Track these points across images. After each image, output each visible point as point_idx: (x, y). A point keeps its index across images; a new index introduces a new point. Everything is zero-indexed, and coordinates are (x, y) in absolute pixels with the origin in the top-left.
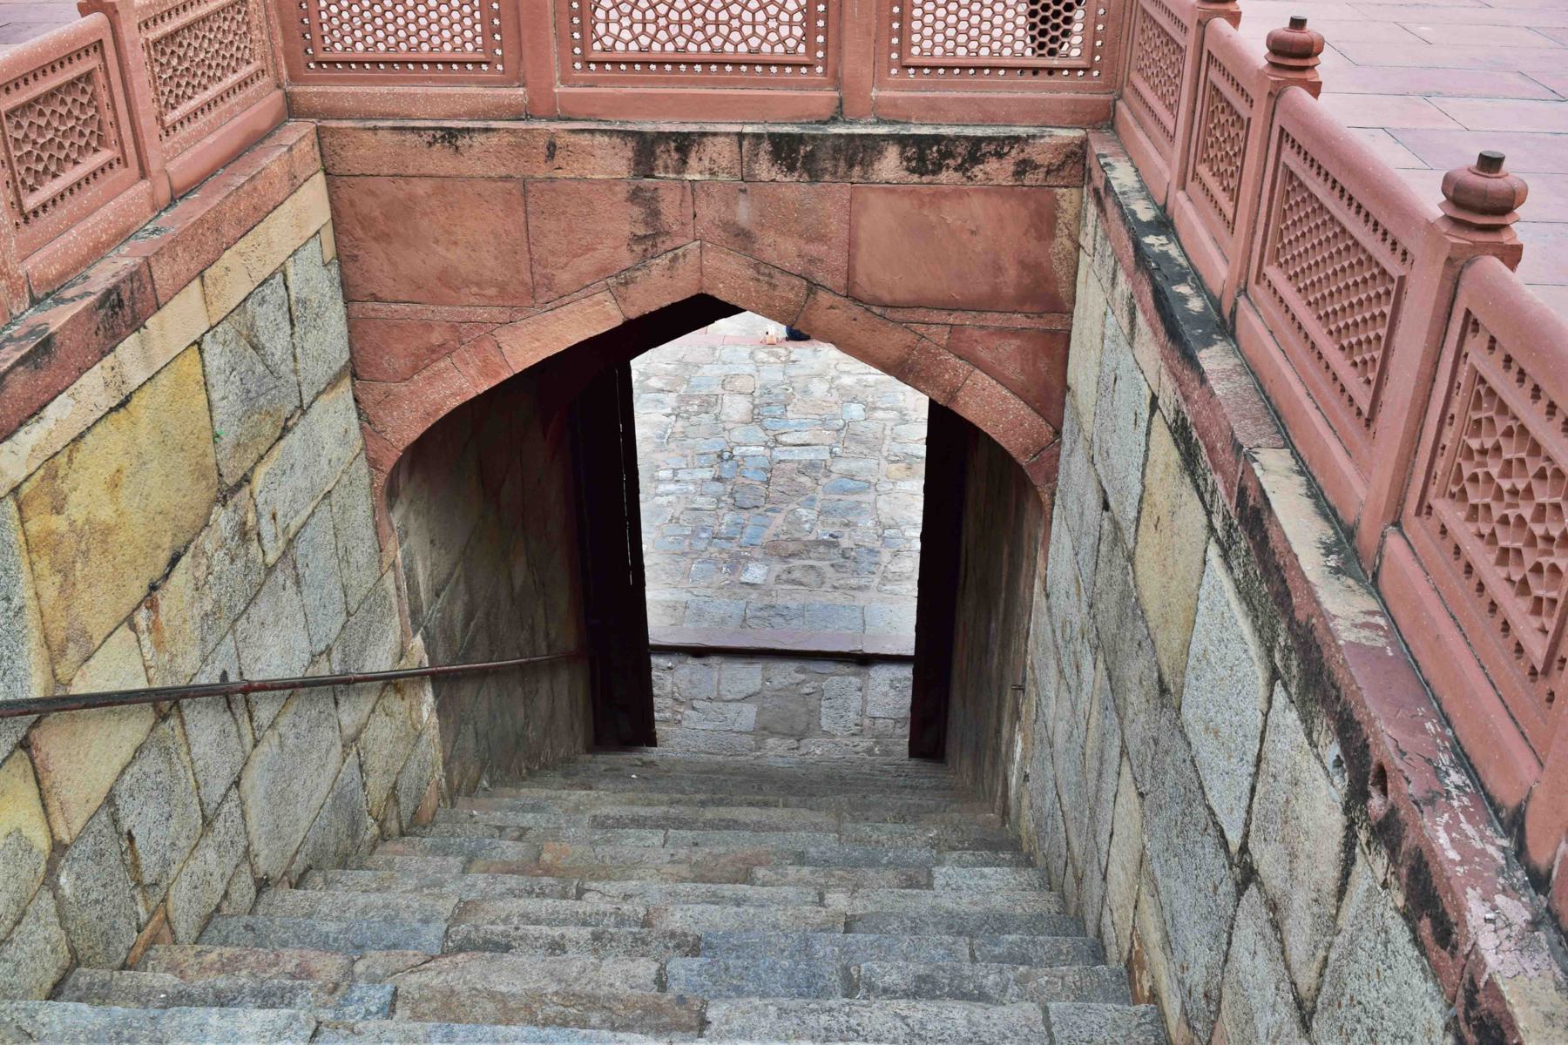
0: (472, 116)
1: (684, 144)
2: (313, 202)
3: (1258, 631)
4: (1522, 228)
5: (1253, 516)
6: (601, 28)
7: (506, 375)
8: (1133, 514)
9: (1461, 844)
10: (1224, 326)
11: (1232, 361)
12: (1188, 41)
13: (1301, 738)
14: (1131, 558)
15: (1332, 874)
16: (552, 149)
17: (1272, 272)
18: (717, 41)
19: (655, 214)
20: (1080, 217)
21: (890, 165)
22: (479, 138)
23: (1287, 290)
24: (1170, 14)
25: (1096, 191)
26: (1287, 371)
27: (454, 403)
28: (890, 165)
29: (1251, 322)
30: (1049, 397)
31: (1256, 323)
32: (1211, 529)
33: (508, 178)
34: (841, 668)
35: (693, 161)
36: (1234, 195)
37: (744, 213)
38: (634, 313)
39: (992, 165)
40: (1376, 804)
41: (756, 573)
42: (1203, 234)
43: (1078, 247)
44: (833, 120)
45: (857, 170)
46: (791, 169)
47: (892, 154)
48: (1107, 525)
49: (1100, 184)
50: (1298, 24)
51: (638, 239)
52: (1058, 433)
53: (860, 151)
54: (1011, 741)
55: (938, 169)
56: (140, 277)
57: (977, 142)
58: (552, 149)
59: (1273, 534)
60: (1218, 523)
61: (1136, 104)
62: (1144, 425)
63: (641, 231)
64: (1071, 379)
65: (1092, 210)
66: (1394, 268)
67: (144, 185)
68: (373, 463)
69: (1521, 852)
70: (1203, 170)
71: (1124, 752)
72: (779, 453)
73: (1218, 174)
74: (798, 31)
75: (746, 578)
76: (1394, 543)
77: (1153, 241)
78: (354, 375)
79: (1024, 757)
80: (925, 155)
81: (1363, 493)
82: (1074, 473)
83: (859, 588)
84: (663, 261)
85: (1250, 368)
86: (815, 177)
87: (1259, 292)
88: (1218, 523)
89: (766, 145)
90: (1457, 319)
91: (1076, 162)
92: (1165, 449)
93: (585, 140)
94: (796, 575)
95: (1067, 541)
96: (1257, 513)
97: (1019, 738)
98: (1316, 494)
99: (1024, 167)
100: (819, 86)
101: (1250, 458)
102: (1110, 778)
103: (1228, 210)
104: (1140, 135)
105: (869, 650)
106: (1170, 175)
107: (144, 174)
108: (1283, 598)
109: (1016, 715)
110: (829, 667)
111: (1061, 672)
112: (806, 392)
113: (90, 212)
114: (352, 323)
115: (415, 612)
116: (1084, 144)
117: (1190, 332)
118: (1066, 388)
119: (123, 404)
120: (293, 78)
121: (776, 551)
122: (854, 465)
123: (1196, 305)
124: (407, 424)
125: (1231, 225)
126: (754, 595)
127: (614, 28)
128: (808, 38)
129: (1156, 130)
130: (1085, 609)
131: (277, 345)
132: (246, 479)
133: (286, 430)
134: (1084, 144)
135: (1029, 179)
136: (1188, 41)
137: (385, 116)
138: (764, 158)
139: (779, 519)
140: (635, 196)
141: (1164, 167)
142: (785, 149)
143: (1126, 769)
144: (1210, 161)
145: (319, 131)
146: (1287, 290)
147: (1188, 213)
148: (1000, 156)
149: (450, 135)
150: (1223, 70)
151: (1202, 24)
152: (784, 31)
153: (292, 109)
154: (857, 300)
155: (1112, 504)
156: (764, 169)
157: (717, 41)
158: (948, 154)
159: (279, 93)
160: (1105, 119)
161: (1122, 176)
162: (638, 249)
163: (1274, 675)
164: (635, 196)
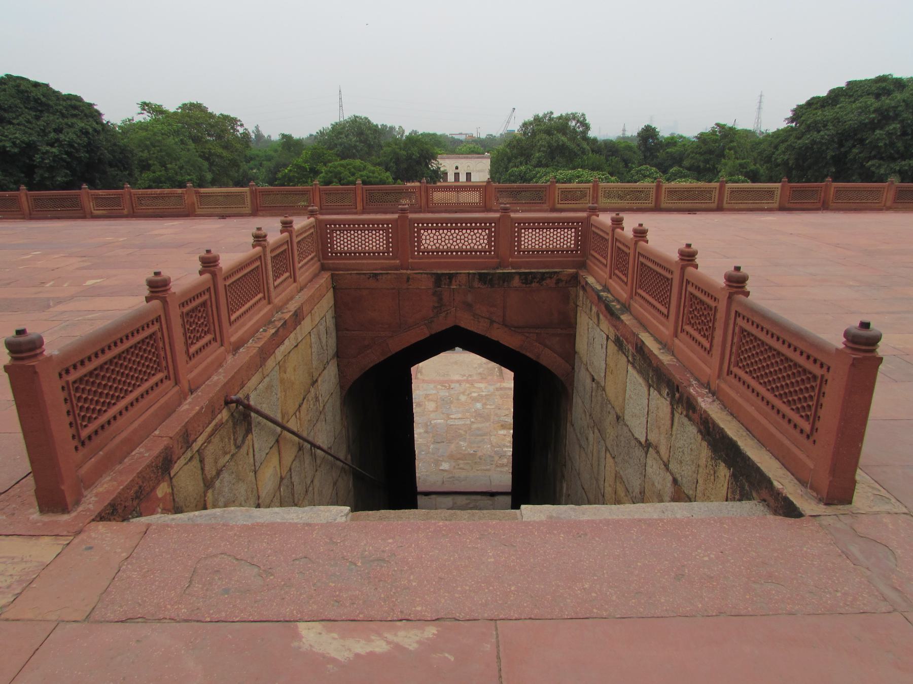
0: (382, 269)
1: (451, 277)
2: (329, 297)
3: (644, 379)
4: (698, 260)
5: (641, 348)
6: (424, 242)
7: (389, 354)
8: (603, 375)
9: (697, 392)
10: (626, 308)
11: (630, 317)
12: (609, 237)
13: (659, 396)
14: (604, 390)
15: (669, 423)
16: (408, 279)
17: (640, 291)
18: (460, 245)
19: (440, 299)
20: (577, 296)
21: (516, 282)
22: (384, 276)
23: (644, 294)
24: (602, 230)
25: (583, 287)
26: (646, 314)
27: (371, 365)
28: (516, 282)
29: (636, 306)
30: (570, 354)
31: (636, 305)
32: (629, 361)
33: (394, 289)
34: (484, 497)
35: (453, 282)
36: (626, 275)
37: (470, 298)
38: (433, 332)
39: (548, 281)
40: (677, 395)
41: (445, 466)
42: (618, 288)
43: (577, 306)
44: (497, 268)
45: (506, 284)
46: (485, 284)
47: (517, 278)
48: (594, 385)
49: (583, 283)
50: (641, 225)
51: (435, 308)
52: (573, 368)
53: (507, 277)
54: (562, 488)
55: (531, 282)
56: (300, 308)
57: (544, 273)
58: (408, 279)
59: (646, 350)
60: (630, 359)
61: (593, 259)
62: (604, 347)
63: (436, 305)
64: (577, 349)
65: (581, 293)
66: (669, 276)
67: (295, 284)
68: (342, 387)
69: (710, 389)
70: (617, 272)
71: (607, 449)
72: (450, 422)
73: (621, 272)
74: (486, 241)
75: (441, 468)
76: (676, 341)
77: (604, 294)
78: (338, 357)
79: (567, 489)
80: (527, 278)
81: (666, 331)
82: (582, 379)
83: (487, 470)
84: (443, 314)
85: (636, 318)
86: (492, 286)
87: (637, 298)
88: (630, 359)
89: (477, 276)
90: (685, 281)
91: (575, 280)
92: (612, 347)
93: (419, 276)
94: (461, 466)
95: (580, 401)
96: (641, 348)
97: (565, 485)
98: (656, 340)
99: (558, 281)
100: (493, 258)
101: (637, 335)
102: (603, 460)
103: (625, 280)
104: (596, 268)
105: (494, 490)
106: (606, 276)
107: (295, 281)
108: (650, 364)
109: (563, 476)
110: (479, 497)
111: (580, 446)
112: (458, 399)
113: (285, 290)
114: (338, 338)
115: (349, 447)
116: (577, 273)
117: (618, 313)
118: (575, 352)
119: (296, 346)
120: (324, 258)
121: (451, 457)
122: (480, 425)
123: (618, 307)
124: (354, 374)
125: (626, 284)
126: (445, 474)
127: (428, 242)
128: (489, 243)
129: (600, 265)
130: (588, 417)
131: (324, 340)
132: (317, 381)
133: (325, 368)
134: (577, 273)
135: (560, 285)
136: (609, 237)
137: (353, 270)
138: (476, 280)
139: (453, 446)
140: (434, 294)
141: (604, 274)
142: (483, 278)
143: (608, 455)
144: (618, 269)
145: (332, 276)
146: (644, 294)
147: (614, 284)
148: (551, 278)
149: (376, 275)
150: (620, 242)
151: (613, 230)
152: (482, 241)
153: (323, 268)
154: (506, 326)
155: (596, 377)
156: (476, 284)
157: (460, 245)
158: (535, 278)
159: (319, 263)
160: (583, 265)
161: (591, 280)
162: (435, 311)
163: (649, 386)
164: (434, 294)
